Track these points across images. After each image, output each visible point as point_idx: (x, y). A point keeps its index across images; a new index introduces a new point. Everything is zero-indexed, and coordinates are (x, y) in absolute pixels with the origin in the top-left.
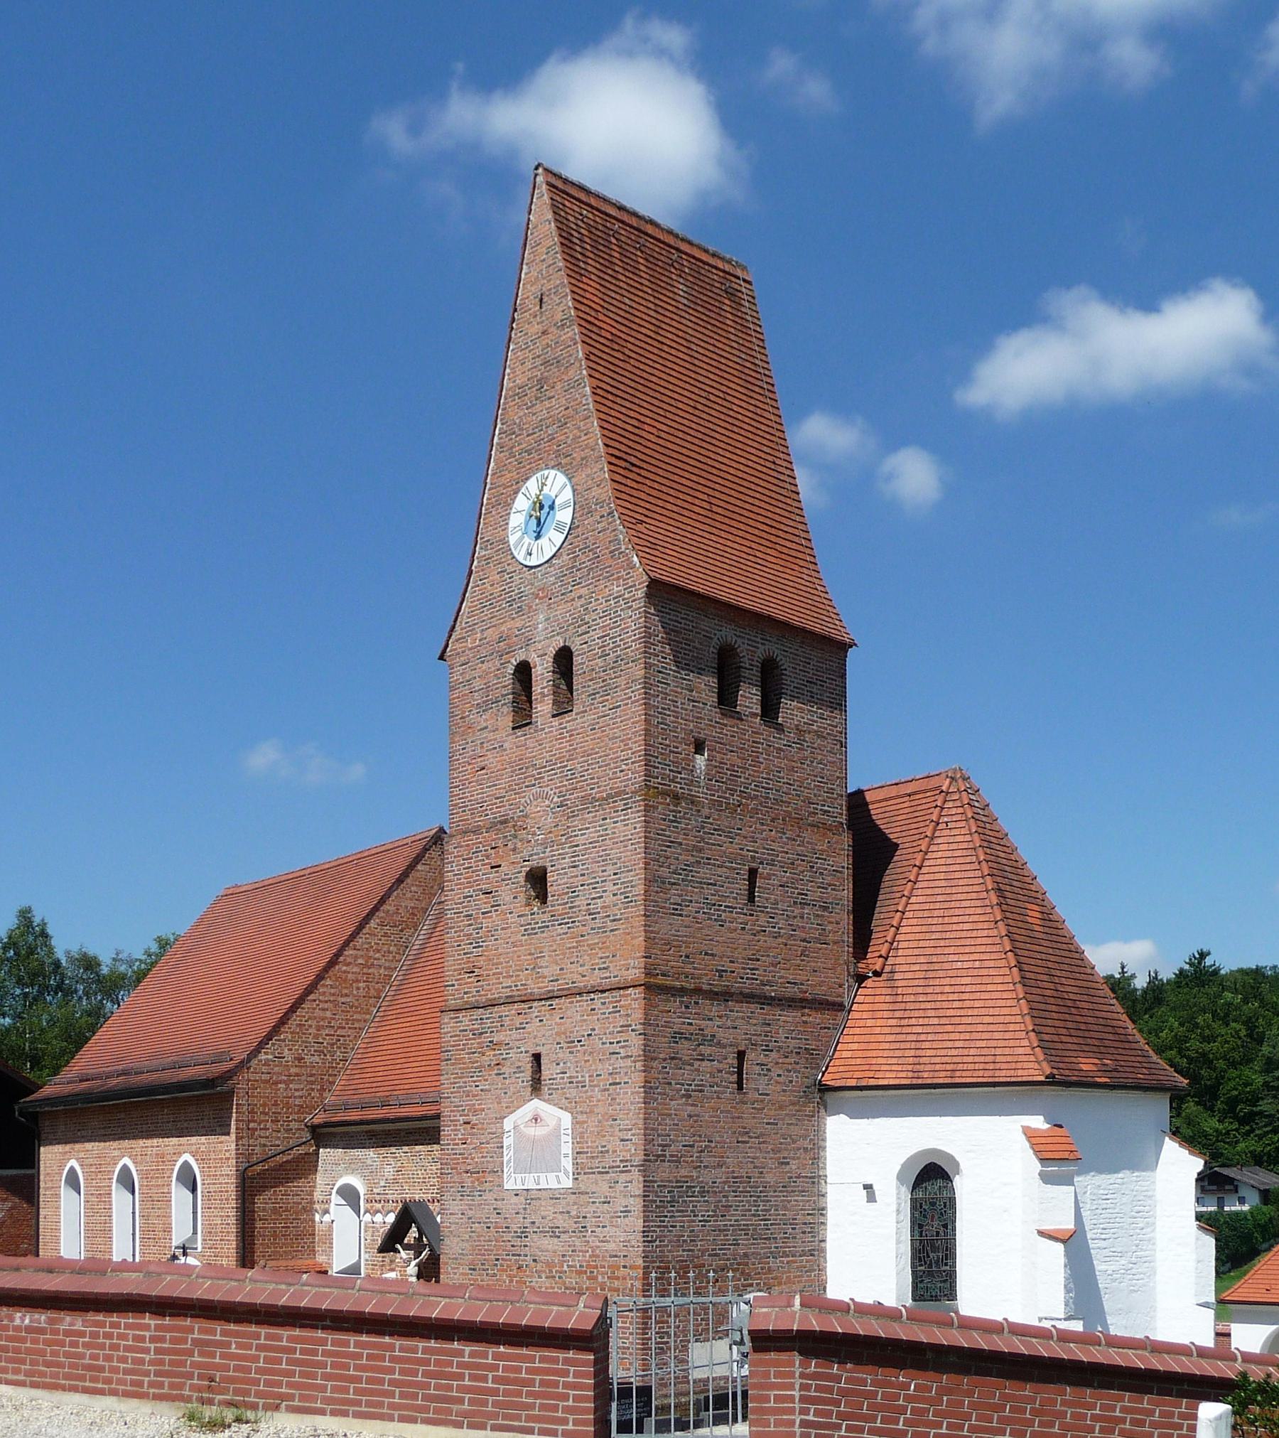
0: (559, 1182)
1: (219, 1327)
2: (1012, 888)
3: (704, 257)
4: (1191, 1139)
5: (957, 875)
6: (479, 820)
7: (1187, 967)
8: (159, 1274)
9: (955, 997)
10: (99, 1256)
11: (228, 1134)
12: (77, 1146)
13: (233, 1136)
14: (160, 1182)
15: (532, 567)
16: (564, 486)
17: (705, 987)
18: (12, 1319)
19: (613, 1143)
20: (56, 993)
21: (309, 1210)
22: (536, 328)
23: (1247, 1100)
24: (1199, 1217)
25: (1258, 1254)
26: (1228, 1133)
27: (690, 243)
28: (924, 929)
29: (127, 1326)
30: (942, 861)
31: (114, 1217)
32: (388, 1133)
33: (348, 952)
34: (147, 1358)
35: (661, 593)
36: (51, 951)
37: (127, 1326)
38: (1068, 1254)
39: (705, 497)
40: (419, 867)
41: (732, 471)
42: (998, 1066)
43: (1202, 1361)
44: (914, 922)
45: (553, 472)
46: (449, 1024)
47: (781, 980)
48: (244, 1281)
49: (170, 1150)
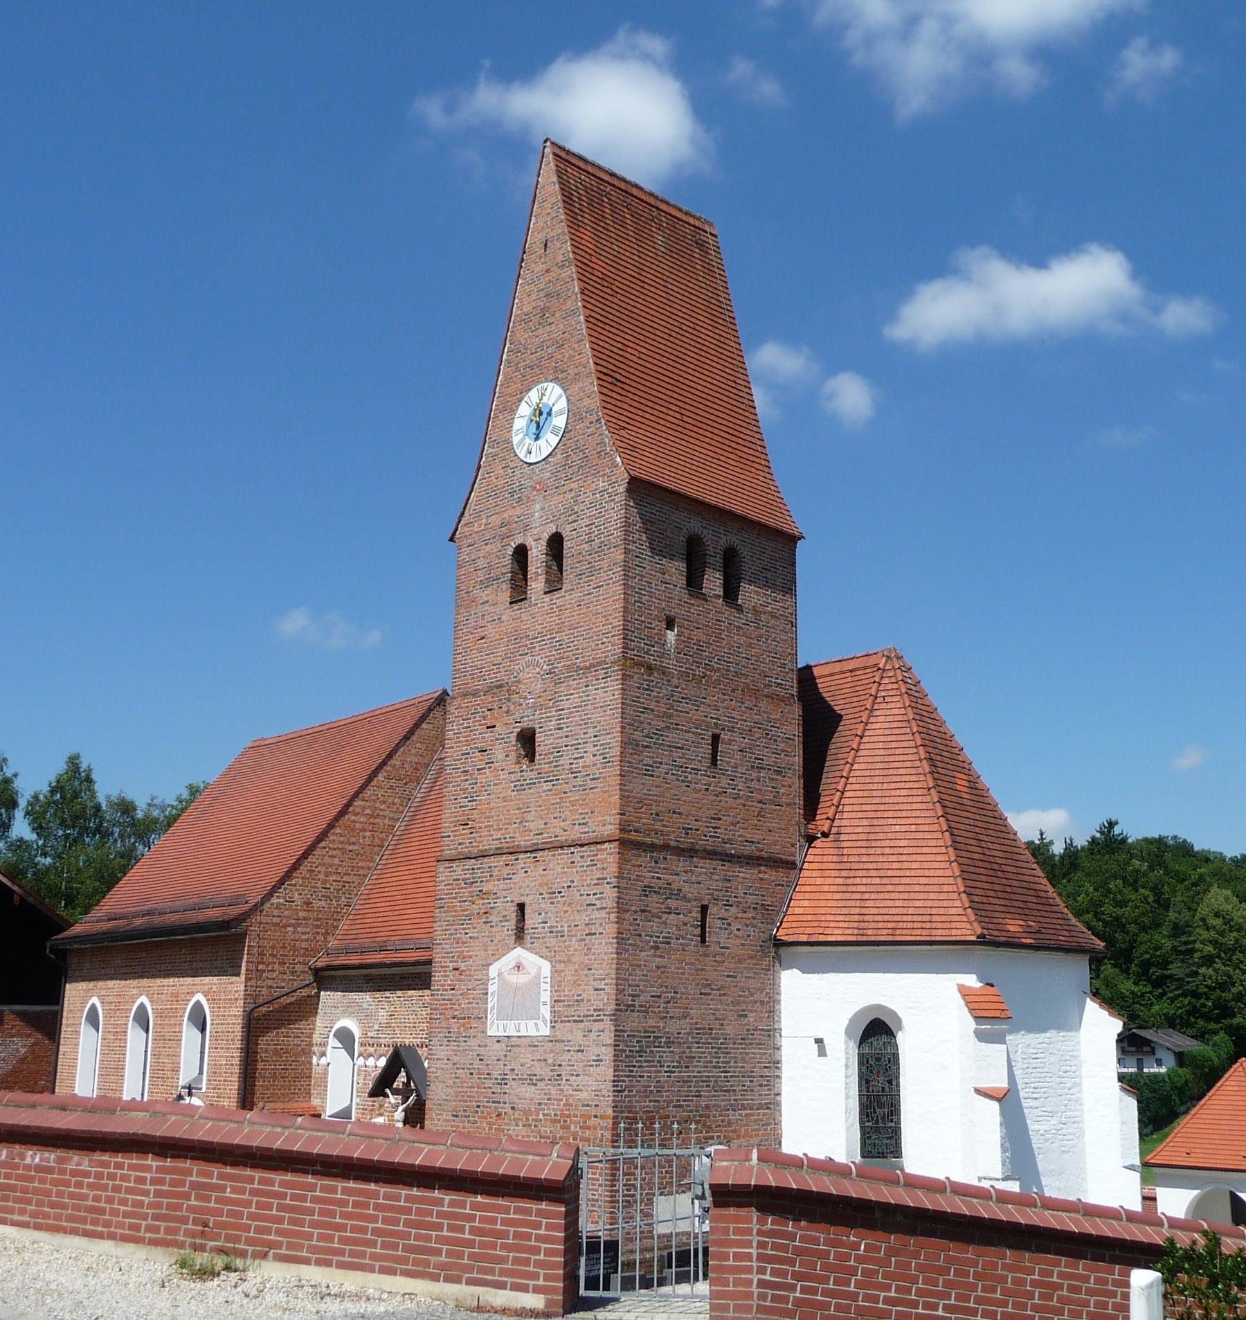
0: (538, 1030)
1: (216, 1170)
2: (942, 758)
3: (679, 215)
4: (1111, 1002)
5: (894, 745)
6: (478, 685)
7: (1098, 835)
8: (165, 1114)
9: (894, 858)
10: (110, 1094)
11: (238, 975)
12: (101, 984)
13: (243, 977)
14: (173, 1021)
15: (531, 464)
16: (560, 397)
17: (673, 844)
18: (23, 1157)
19: (588, 993)
20: (94, 835)
21: (308, 1053)
22: (541, 267)
23: (1159, 963)
24: (1121, 1078)
25: (1177, 1117)
26: (1143, 995)
27: (667, 203)
28: (866, 794)
29: (131, 1167)
30: (881, 732)
31: (128, 1056)
32: (383, 977)
33: (358, 803)
34: (146, 1200)
35: (639, 488)
36: (93, 796)
37: (131, 1167)
38: (1003, 1113)
39: (677, 409)
40: (424, 726)
41: (700, 388)
42: (934, 925)
43: (1131, 1226)
44: (857, 787)
45: (551, 385)
46: (444, 874)
47: (740, 838)
48: (242, 1123)
49: (185, 989)
